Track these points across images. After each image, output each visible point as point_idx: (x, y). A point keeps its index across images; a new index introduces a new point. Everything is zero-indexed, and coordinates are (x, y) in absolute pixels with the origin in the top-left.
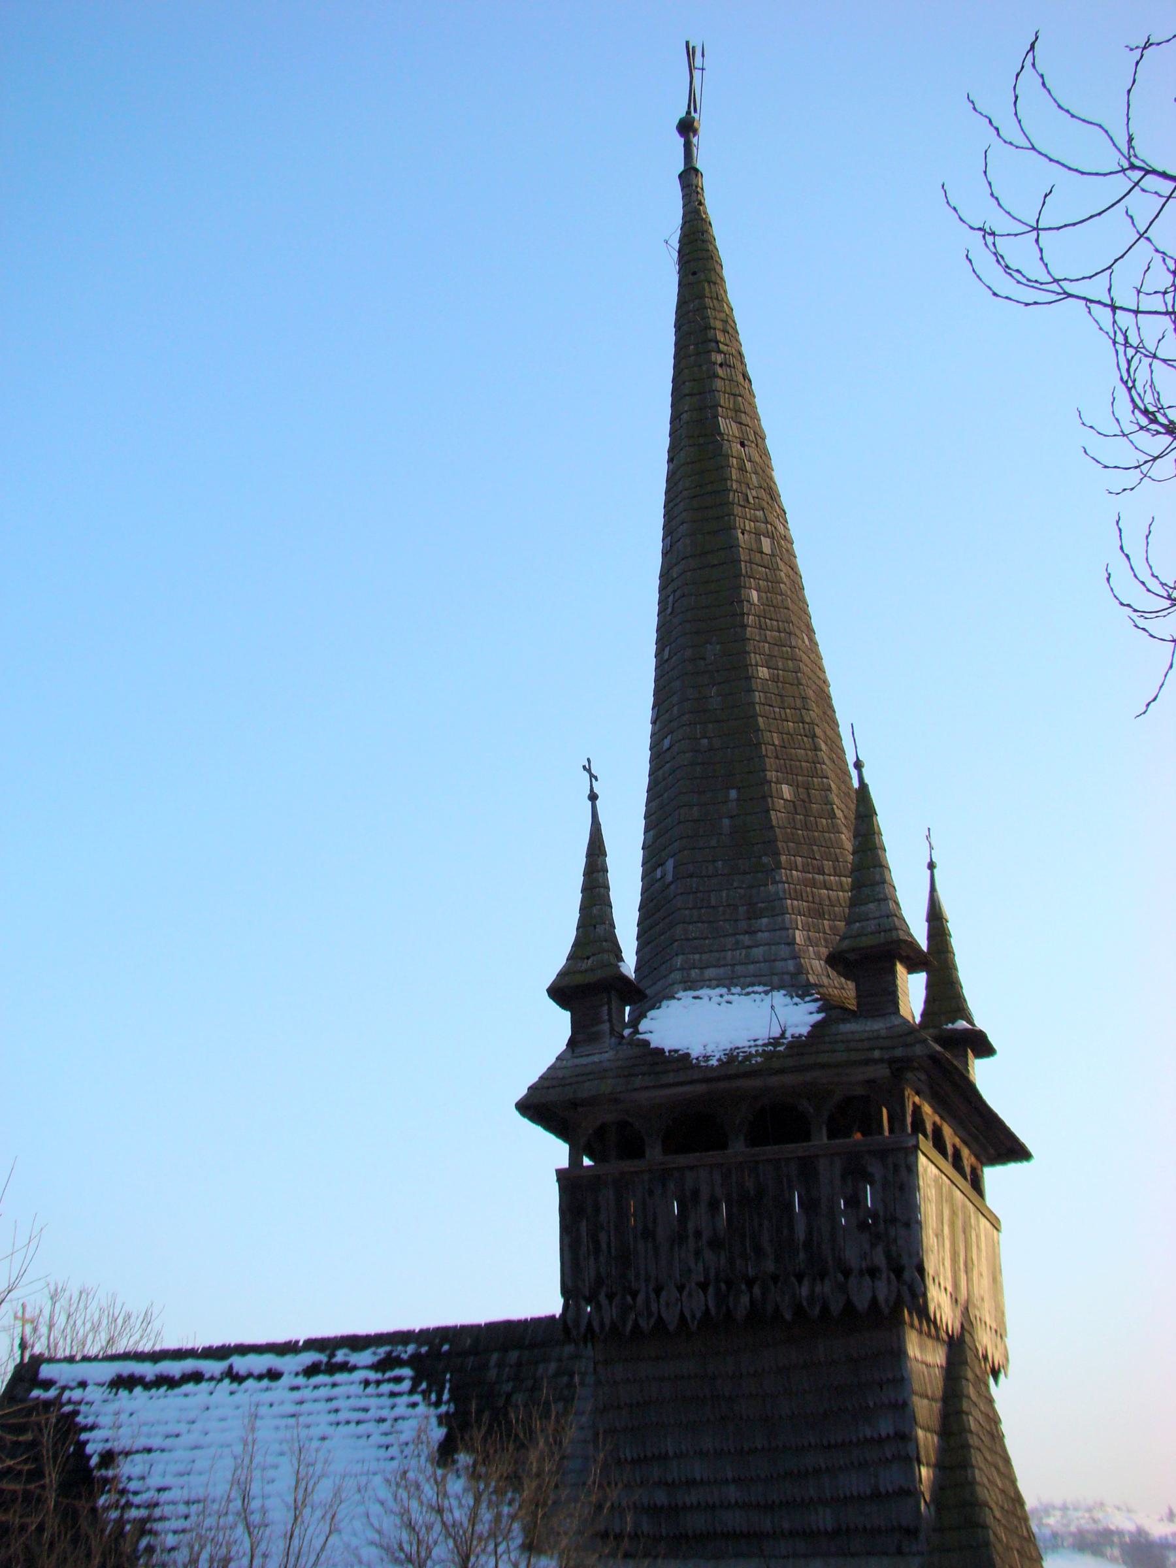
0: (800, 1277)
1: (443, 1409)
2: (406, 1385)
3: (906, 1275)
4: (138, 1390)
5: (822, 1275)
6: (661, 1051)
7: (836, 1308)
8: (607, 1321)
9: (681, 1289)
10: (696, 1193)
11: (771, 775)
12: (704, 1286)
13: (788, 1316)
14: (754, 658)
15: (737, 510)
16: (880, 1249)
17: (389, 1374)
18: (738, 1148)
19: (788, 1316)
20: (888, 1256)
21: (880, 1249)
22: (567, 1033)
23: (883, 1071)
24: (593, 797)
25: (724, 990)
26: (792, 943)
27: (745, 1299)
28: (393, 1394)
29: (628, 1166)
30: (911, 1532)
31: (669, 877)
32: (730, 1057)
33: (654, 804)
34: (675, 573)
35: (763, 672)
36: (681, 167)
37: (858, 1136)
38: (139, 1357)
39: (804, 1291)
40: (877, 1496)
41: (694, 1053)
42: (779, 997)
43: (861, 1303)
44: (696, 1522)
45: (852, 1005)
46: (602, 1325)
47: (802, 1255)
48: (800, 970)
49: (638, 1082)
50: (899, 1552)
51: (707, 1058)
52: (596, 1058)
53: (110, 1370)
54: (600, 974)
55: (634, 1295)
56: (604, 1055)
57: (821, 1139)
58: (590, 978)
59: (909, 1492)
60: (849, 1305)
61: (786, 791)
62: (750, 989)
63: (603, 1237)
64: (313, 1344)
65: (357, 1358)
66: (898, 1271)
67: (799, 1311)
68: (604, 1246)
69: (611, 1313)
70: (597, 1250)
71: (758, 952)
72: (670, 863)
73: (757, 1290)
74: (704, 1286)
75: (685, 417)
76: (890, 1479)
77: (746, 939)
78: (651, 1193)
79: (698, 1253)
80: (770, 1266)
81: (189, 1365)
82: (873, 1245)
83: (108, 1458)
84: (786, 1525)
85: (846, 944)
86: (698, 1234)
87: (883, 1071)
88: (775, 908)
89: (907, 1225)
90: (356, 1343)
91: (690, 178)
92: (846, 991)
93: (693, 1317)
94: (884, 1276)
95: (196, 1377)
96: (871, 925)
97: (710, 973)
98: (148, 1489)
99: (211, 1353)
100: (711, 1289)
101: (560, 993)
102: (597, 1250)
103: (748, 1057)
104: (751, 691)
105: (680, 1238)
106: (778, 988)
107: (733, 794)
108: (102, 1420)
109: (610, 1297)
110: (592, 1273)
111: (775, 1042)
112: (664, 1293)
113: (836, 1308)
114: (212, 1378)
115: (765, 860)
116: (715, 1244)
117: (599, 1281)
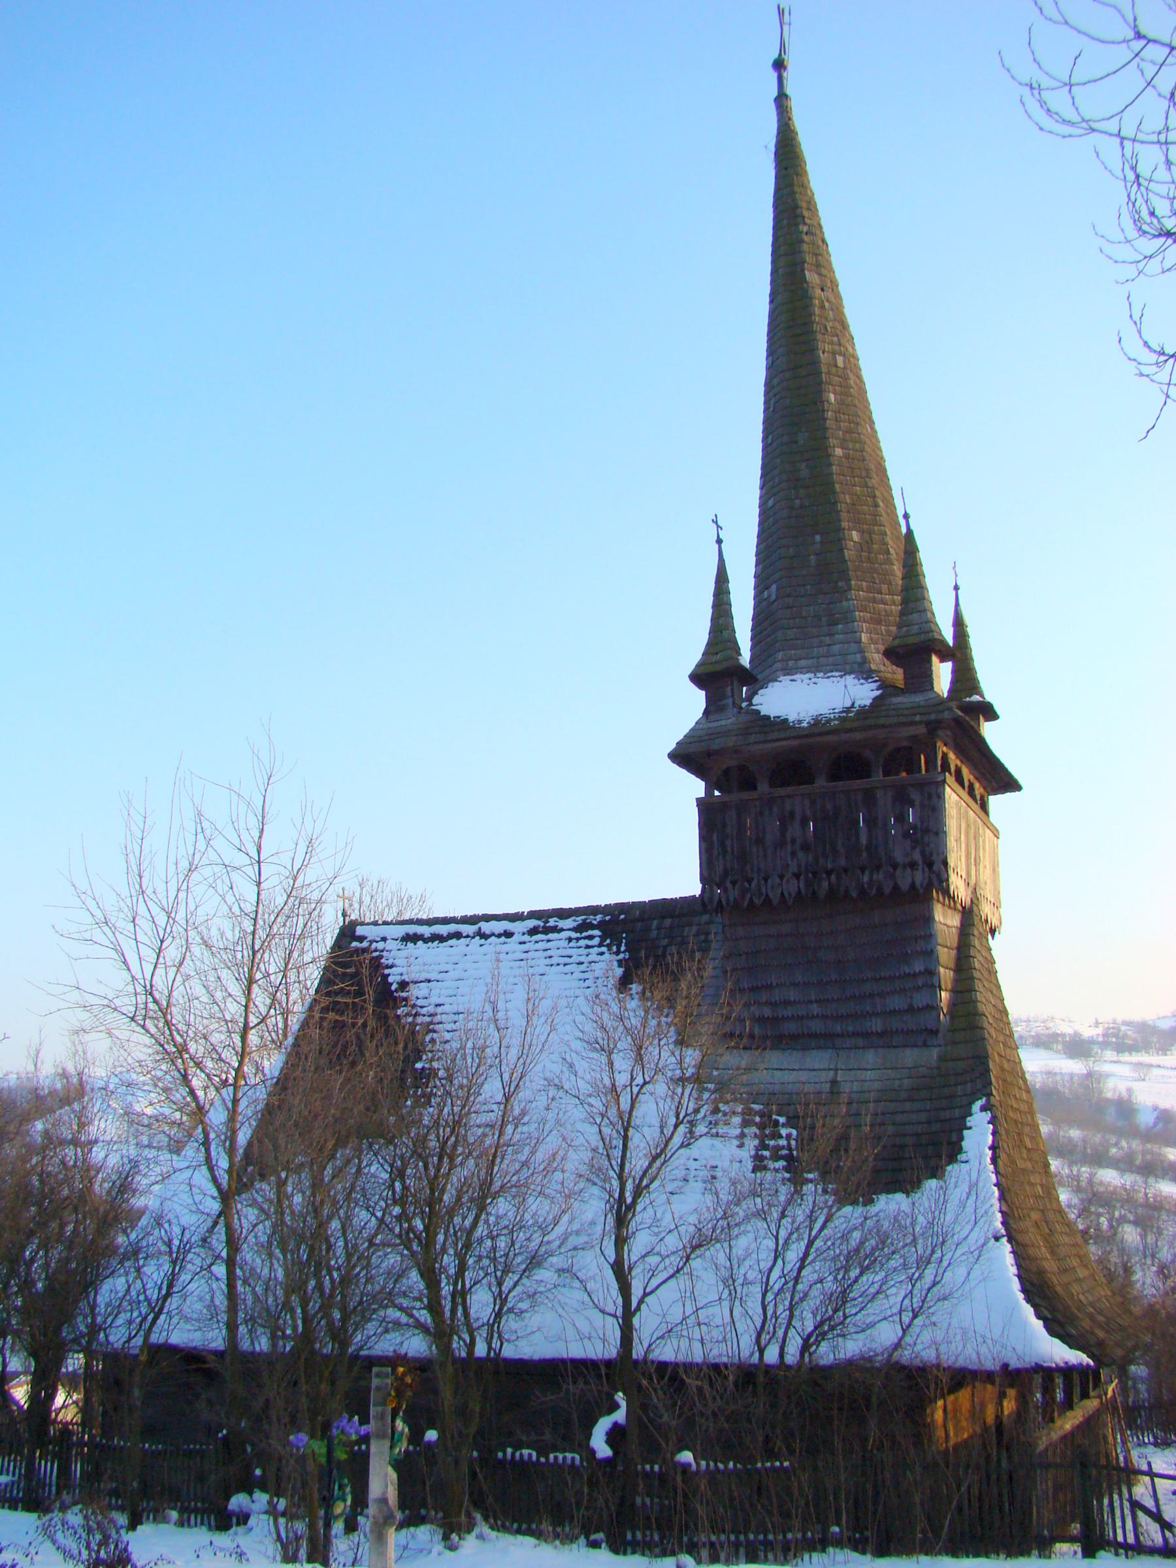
0: (863, 869)
1: (621, 956)
2: (596, 941)
3: (935, 868)
4: (420, 943)
5: (878, 868)
6: (767, 718)
7: (887, 890)
8: (731, 899)
9: (781, 877)
10: (792, 814)
11: (845, 524)
12: (797, 876)
13: (854, 894)
14: (832, 442)
15: (819, 337)
16: (918, 850)
17: (584, 934)
18: (821, 782)
19: (854, 894)
20: (923, 854)
21: (918, 850)
22: (703, 705)
23: (922, 730)
24: (719, 541)
25: (812, 675)
26: (859, 642)
27: (825, 884)
28: (588, 947)
29: (745, 795)
30: (934, 1032)
31: (773, 597)
32: (817, 721)
33: (762, 546)
34: (775, 381)
35: (839, 452)
36: (775, 94)
37: (904, 774)
38: (420, 922)
39: (866, 879)
40: (911, 1010)
41: (791, 719)
42: (850, 680)
43: (904, 885)
44: (791, 1027)
45: (900, 684)
46: (728, 900)
47: (864, 854)
48: (865, 661)
49: (752, 738)
50: (925, 1045)
51: (800, 722)
52: (723, 723)
53: (401, 930)
54: (725, 665)
55: (750, 881)
56: (728, 721)
57: (878, 777)
58: (718, 668)
59: (933, 1008)
60: (896, 888)
61: (855, 535)
62: (830, 674)
63: (728, 842)
64: (533, 915)
65: (563, 924)
66: (930, 865)
67: (863, 892)
68: (729, 849)
69: (734, 893)
70: (725, 852)
71: (836, 648)
72: (774, 587)
73: (833, 877)
74: (797, 876)
75: (781, 271)
76: (920, 1000)
77: (827, 640)
78: (761, 813)
79: (793, 854)
80: (842, 862)
81: (453, 927)
82: (913, 848)
83: (403, 985)
84: (851, 1029)
85: (897, 642)
86: (793, 841)
87: (922, 730)
88: (847, 618)
89: (937, 834)
90: (562, 914)
91: (781, 101)
92: (897, 675)
93: (790, 894)
94: (920, 868)
95: (458, 935)
96: (915, 629)
97: (802, 663)
98: (430, 1005)
99: (466, 920)
100: (802, 877)
101: (699, 678)
102: (725, 852)
103: (829, 721)
104: (830, 465)
105: (781, 844)
106: (850, 673)
107: (818, 538)
108: (397, 962)
109: (734, 883)
110: (722, 867)
111: (847, 710)
112: (770, 881)
113: (887, 890)
114: (468, 936)
115: (840, 584)
116: (805, 847)
117: (726, 872)
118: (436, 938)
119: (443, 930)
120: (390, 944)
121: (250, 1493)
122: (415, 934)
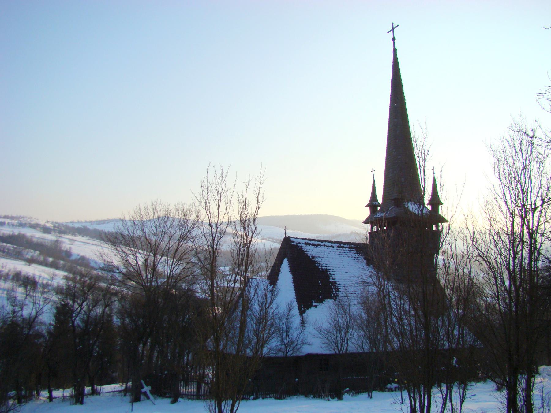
17: (352, 250)
53: (304, 241)
65: (346, 246)
91: (395, 51)
95: (320, 245)
98: (323, 264)
108: (308, 250)
118: (313, 245)
119: (316, 243)
120: (303, 245)
121: (391, 384)
122: (308, 243)
